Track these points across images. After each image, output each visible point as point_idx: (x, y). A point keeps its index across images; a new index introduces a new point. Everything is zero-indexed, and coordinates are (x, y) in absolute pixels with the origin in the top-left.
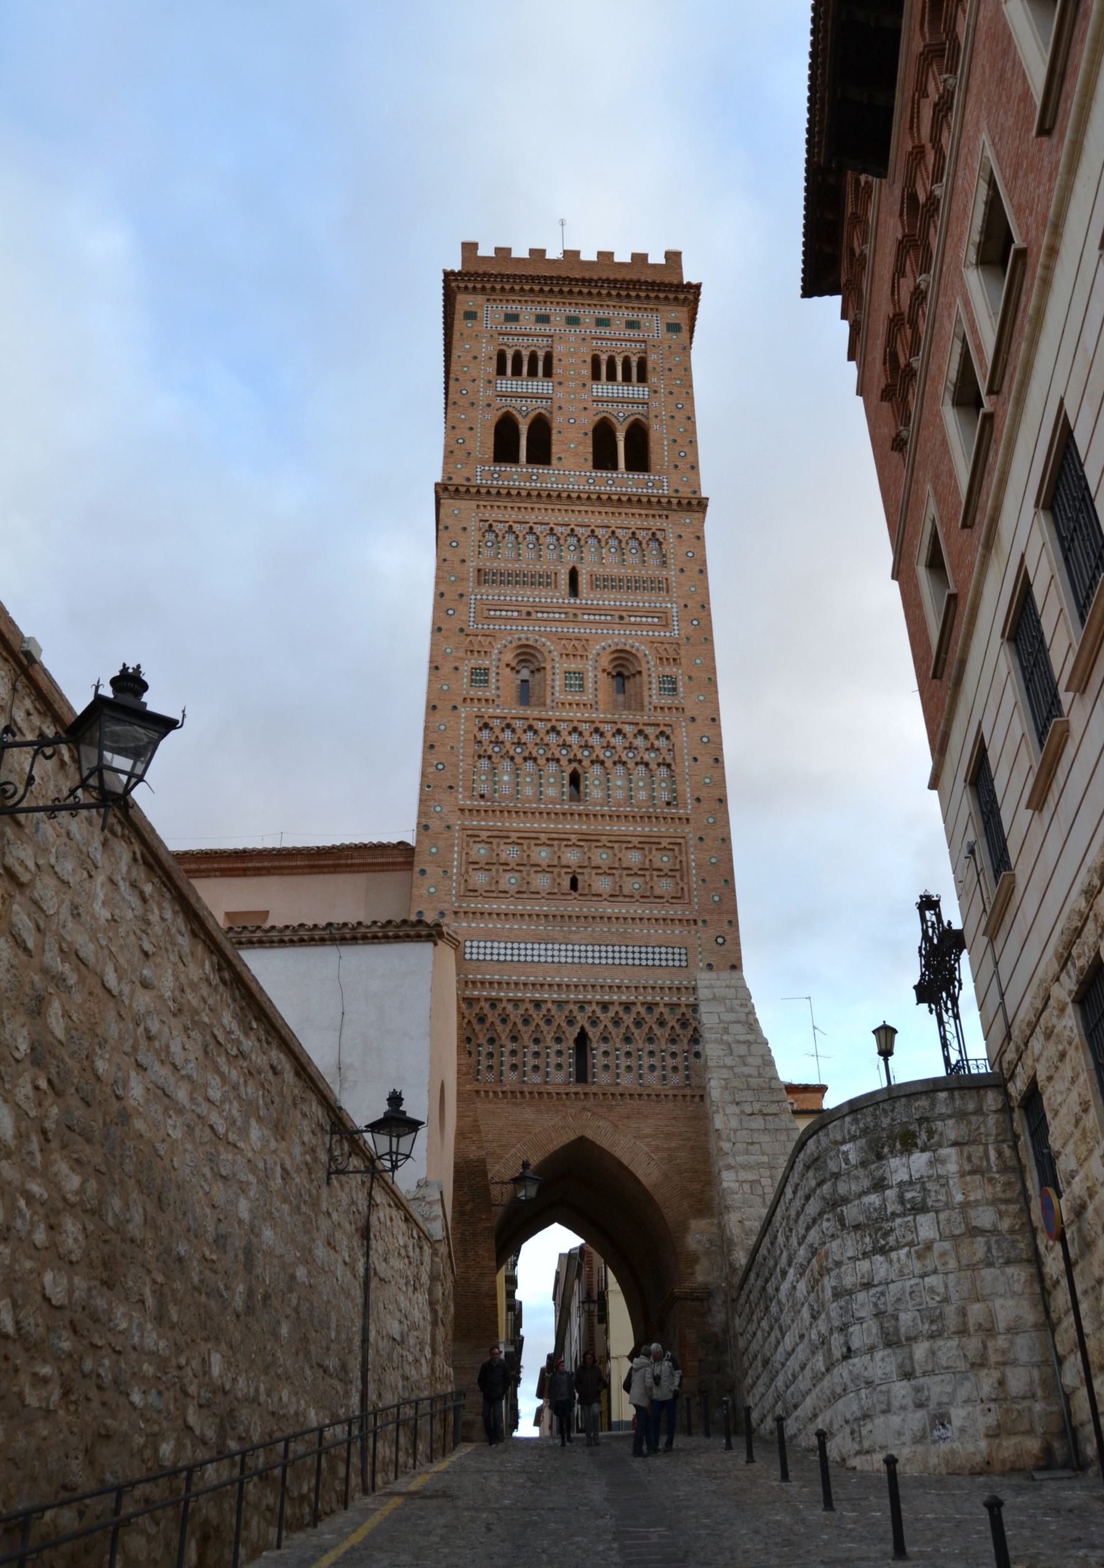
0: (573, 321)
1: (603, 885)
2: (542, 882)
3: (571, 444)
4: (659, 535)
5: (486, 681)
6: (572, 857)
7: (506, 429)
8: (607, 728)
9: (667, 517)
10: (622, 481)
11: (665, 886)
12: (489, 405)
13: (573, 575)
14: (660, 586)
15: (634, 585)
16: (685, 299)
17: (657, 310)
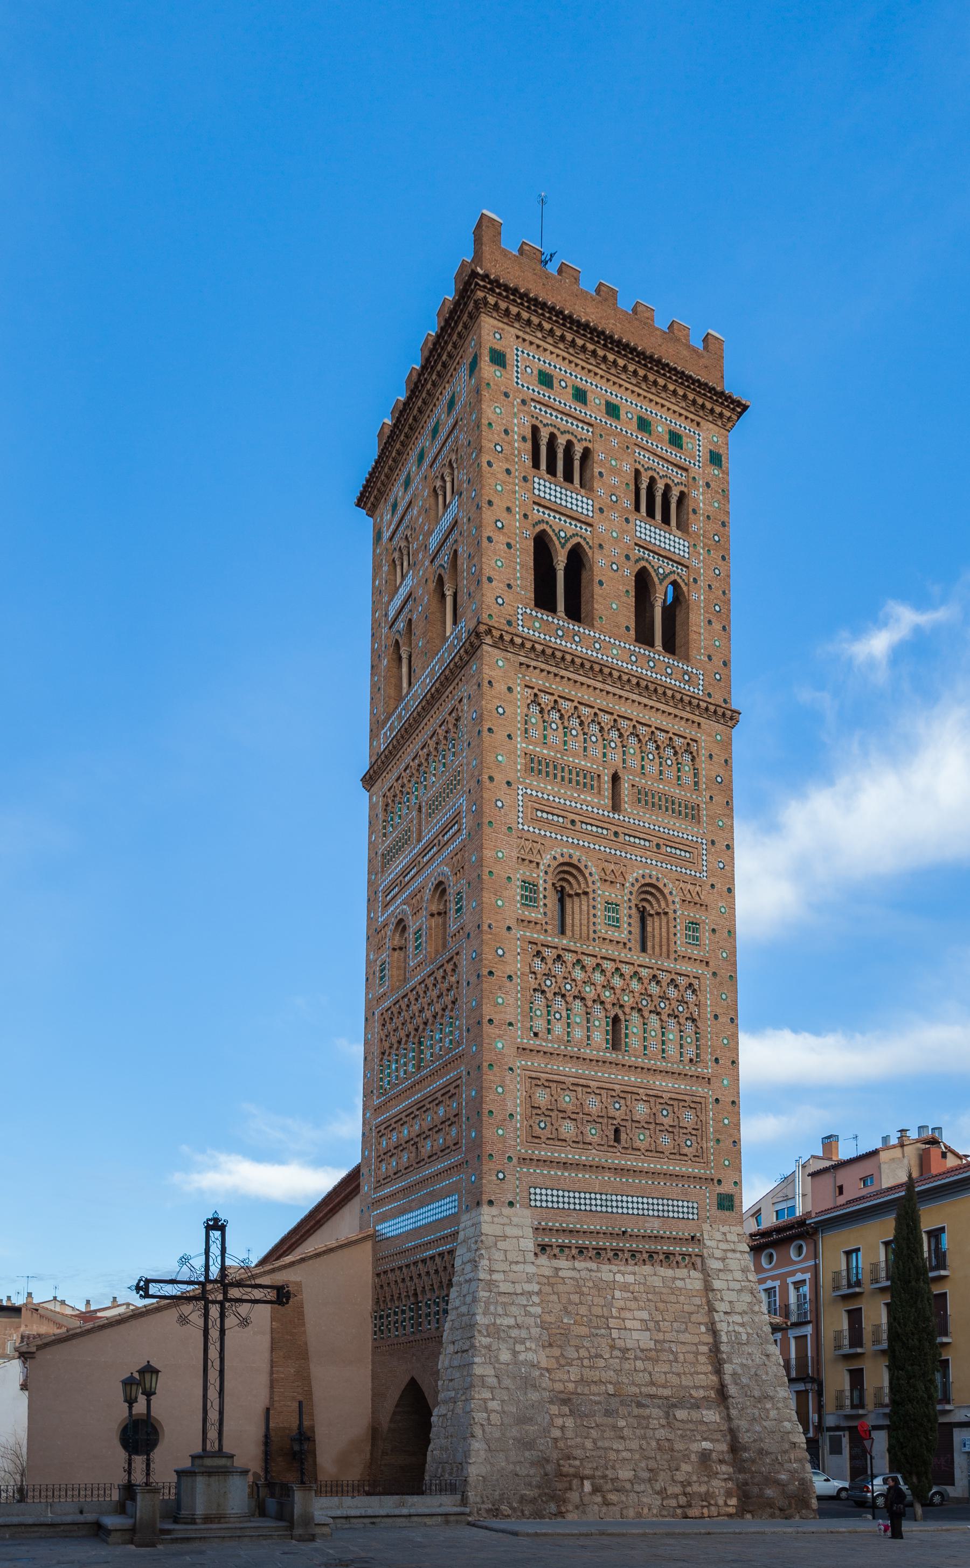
2: (592, 1134)
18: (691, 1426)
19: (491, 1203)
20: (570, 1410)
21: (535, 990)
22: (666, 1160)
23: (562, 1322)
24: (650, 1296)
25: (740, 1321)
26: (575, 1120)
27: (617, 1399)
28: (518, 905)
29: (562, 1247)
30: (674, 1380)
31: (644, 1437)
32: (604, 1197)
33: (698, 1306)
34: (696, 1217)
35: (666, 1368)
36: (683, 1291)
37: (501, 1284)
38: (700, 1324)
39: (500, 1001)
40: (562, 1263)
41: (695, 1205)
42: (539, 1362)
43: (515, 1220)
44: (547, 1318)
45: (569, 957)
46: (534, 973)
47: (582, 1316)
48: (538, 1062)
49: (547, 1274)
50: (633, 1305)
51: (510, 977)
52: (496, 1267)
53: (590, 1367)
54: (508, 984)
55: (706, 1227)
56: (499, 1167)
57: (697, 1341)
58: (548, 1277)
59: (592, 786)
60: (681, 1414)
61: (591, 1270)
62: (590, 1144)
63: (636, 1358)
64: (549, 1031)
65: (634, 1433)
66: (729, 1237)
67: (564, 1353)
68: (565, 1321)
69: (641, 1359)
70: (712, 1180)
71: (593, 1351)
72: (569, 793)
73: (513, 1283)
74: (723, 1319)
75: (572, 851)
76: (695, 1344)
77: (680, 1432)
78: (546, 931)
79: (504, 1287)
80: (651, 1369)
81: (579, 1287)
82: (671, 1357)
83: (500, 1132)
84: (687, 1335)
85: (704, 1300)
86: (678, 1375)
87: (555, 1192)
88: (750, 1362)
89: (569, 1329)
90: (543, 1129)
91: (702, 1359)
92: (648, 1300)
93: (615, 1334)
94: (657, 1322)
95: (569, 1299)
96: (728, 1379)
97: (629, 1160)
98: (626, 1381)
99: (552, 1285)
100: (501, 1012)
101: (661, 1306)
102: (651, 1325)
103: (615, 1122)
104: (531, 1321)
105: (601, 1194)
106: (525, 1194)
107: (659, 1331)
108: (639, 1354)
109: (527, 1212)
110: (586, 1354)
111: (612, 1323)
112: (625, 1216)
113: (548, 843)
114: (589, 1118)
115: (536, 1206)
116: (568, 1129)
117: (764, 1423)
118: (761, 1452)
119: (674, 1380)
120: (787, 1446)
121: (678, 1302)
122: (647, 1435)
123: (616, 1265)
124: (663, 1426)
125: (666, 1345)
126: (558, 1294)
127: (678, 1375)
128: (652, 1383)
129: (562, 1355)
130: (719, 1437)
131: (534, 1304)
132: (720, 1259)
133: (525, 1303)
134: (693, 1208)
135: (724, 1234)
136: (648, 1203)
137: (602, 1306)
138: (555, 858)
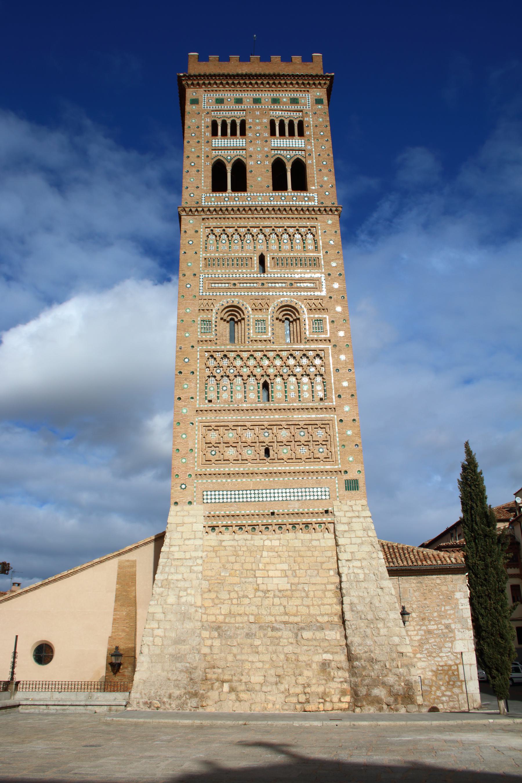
0: (257, 101)
1: (285, 452)
2: (248, 453)
3: (259, 175)
4: (313, 230)
5: (211, 329)
6: (266, 437)
7: (218, 168)
8: (284, 354)
9: (316, 218)
10: (290, 197)
11: (321, 451)
12: (208, 156)
14: (314, 263)
16: (325, 84)
17: (308, 91)
18: (315, 643)
19: (176, 503)
20: (219, 635)
21: (209, 377)
22: (304, 462)
23: (220, 575)
24: (290, 554)
25: (359, 565)
26: (236, 447)
27: (257, 626)
28: (199, 334)
30: (304, 610)
31: (275, 652)
32: (256, 492)
33: (329, 557)
34: (328, 497)
35: (298, 602)
36: (317, 548)
37: (176, 554)
38: (329, 570)
39: (186, 386)
40: (227, 536)
41: (327, 490)
42: (195, 603)
43: (192, 512)
44: (209, 573)
45: (232, 355)
46: (209, 367)
47: (236, 570)
48: (210, 417)
49: (213, 544)
50: (276, 560)
51: (193, 373)
52: (173, 543)
53: (238, 604)
54: (191, 376)
55: (336, 503)
56: (182, 482)
57: (325, 581)
58: (214, 547)
59: (247, 264)
60: (307, 634)
61: (246, 540)
62: (247, 460)
63: (275, 596)
64: (218, 397)
65: (267, 650)
67: (219, 596)
68: (222, 574)
69: (278, 597)
70: (340, 471)
71: (241, 594)
72: (231, 271)
73: (185, 552)
74: (344, 564)
75: (233, 299)
76: (325, 584)
77: (305, 648)
78: (216, 343)
79: (177, 556)
80: (285, 603)
81: (235, 551)
82: (304, 594)
83: (184, 461)
84: (318, 578)
85: (335, 552)
86: (308, 606)
87: (221, 493)
88: (366, 594)
89: (225, 580)
90: (213, 455)
91: (329, 594)
92: (289, 556)
93: (260, 581)
94: (295, 571)
95: (228, 559)
96: (346, 607)
97: (275, 466)
98: (264, 613)
99: (216, 552)
100: (186, 393)
101: (299, 559)
102: (289, 573)
103: (264, 444)
104: (194, 576)
105: (254, 490)
106: (200, 496)
107: (296, 576)
108: (277, 593)
109: (201, 507)
110: (236, 596)
112: (272, 502)
113: (218, 298)
114: (245, 444)
115: (207, 503)
116: (231, 453)
117: (375, 638)
118: (372, 661)
120: (394, 655)
121: (313, 556)
122: (278, 651)
123: (266, 535)
124: (292, 643)
125: (300, 587)
126: (219, 557)
127: (308, 606)
128: (286, 614)
129: (217, 596)
130: (338, 650)
131: (198, 565)
132: (345, 523)
133: (191, 564)
134: (325, 491)
135: (351, 506)
136: (290, 492)
137: (252, 563)
138: (223, 305)
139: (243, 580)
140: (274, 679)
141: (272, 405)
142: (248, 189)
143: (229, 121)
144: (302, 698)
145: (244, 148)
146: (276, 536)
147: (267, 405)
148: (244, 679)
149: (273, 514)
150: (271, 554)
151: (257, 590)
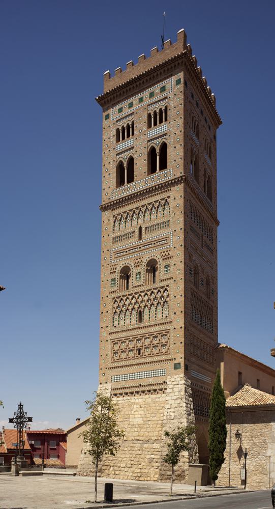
2: (131, 354)
7: (120, 167)
13: (140, 229)
15: (159, 226)
29: (121, 394)
30: (147, 434)
35: (145, 430)
40: (121, 398)
48: (114, 336)
56: (103, 372)
60: (146, 446)
66: (177, 380)
71: (122, 426)
80: (139, 430)
82: (148, 426)
86: (149, 432)
98: (130, 435)
108: (137, 426)
109: (111, 384)
111: (131, 416)
116: (124, 355)
119: (147, 434)
127: (149, 432)
128: (139, 436)
135: (176, 378)
139: (125, 420)
140: (130, 466)
141: (143, 325)
142: (134, 180)
143: (125, 126)
144: (139, 475)
145: (132, 146)
146: (141, 397)
147: (140, 326)
148: (119, 465)
149: (140, 385)
150: (138, 406)
151: (129, 424)
